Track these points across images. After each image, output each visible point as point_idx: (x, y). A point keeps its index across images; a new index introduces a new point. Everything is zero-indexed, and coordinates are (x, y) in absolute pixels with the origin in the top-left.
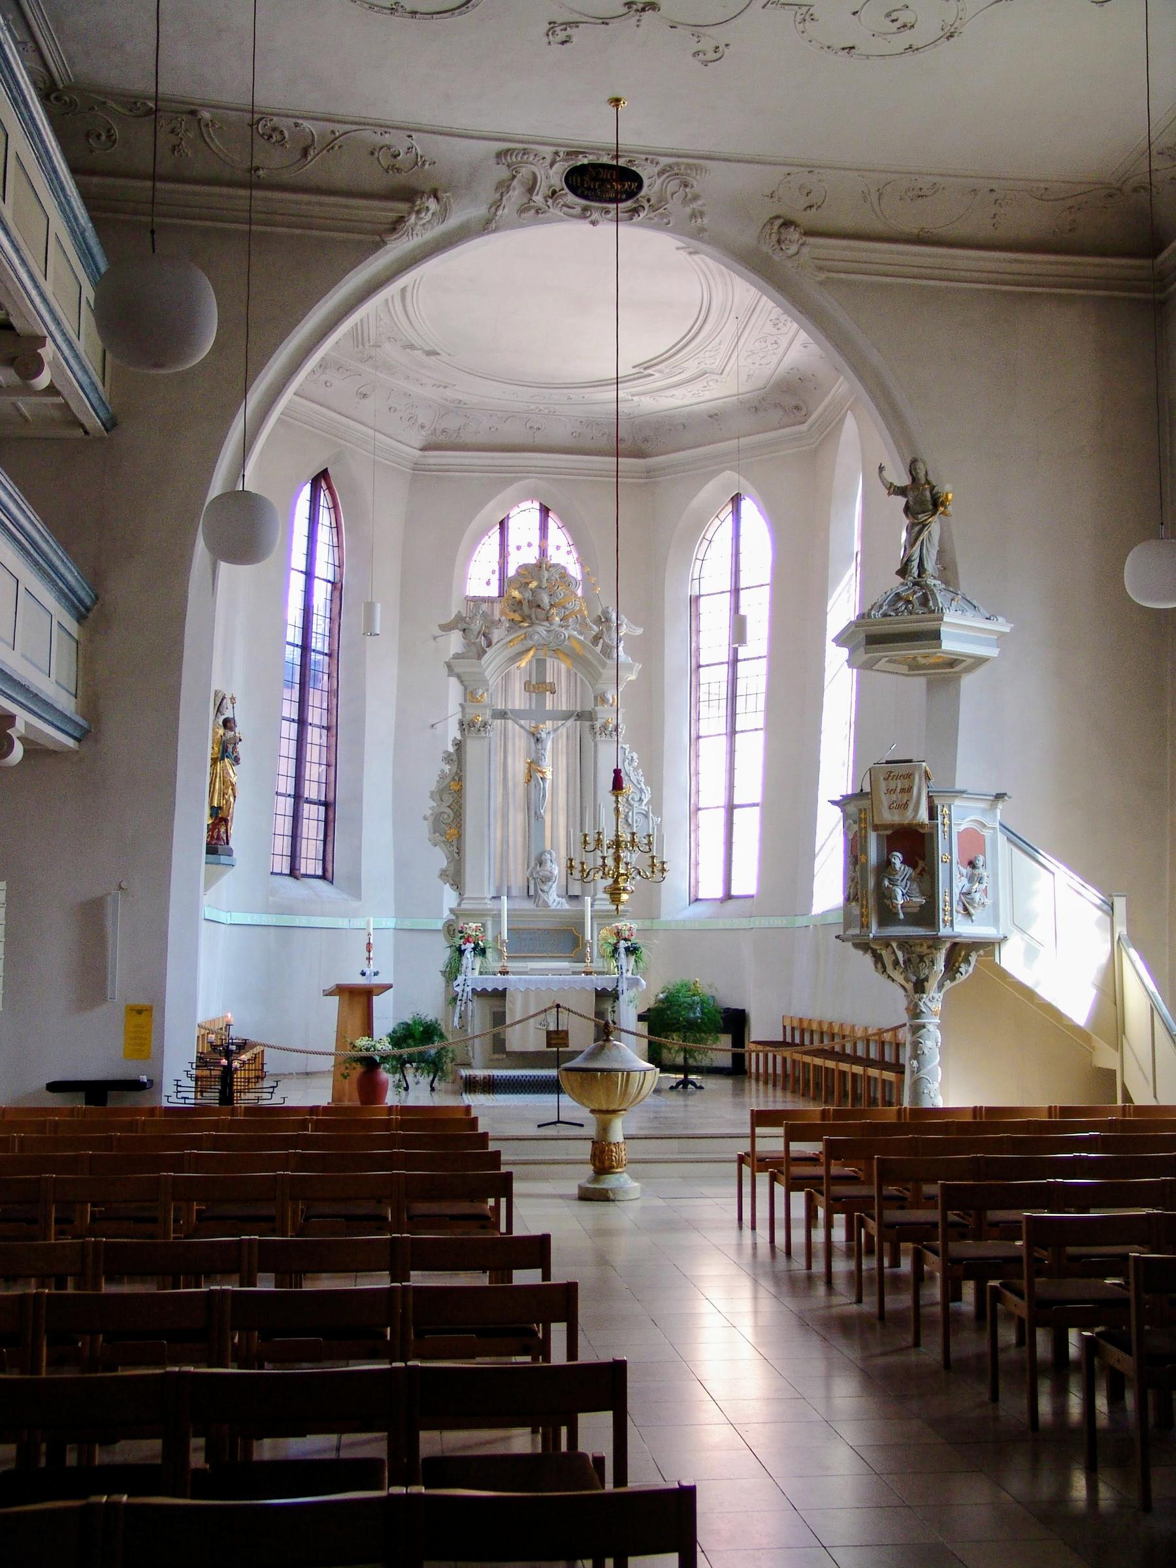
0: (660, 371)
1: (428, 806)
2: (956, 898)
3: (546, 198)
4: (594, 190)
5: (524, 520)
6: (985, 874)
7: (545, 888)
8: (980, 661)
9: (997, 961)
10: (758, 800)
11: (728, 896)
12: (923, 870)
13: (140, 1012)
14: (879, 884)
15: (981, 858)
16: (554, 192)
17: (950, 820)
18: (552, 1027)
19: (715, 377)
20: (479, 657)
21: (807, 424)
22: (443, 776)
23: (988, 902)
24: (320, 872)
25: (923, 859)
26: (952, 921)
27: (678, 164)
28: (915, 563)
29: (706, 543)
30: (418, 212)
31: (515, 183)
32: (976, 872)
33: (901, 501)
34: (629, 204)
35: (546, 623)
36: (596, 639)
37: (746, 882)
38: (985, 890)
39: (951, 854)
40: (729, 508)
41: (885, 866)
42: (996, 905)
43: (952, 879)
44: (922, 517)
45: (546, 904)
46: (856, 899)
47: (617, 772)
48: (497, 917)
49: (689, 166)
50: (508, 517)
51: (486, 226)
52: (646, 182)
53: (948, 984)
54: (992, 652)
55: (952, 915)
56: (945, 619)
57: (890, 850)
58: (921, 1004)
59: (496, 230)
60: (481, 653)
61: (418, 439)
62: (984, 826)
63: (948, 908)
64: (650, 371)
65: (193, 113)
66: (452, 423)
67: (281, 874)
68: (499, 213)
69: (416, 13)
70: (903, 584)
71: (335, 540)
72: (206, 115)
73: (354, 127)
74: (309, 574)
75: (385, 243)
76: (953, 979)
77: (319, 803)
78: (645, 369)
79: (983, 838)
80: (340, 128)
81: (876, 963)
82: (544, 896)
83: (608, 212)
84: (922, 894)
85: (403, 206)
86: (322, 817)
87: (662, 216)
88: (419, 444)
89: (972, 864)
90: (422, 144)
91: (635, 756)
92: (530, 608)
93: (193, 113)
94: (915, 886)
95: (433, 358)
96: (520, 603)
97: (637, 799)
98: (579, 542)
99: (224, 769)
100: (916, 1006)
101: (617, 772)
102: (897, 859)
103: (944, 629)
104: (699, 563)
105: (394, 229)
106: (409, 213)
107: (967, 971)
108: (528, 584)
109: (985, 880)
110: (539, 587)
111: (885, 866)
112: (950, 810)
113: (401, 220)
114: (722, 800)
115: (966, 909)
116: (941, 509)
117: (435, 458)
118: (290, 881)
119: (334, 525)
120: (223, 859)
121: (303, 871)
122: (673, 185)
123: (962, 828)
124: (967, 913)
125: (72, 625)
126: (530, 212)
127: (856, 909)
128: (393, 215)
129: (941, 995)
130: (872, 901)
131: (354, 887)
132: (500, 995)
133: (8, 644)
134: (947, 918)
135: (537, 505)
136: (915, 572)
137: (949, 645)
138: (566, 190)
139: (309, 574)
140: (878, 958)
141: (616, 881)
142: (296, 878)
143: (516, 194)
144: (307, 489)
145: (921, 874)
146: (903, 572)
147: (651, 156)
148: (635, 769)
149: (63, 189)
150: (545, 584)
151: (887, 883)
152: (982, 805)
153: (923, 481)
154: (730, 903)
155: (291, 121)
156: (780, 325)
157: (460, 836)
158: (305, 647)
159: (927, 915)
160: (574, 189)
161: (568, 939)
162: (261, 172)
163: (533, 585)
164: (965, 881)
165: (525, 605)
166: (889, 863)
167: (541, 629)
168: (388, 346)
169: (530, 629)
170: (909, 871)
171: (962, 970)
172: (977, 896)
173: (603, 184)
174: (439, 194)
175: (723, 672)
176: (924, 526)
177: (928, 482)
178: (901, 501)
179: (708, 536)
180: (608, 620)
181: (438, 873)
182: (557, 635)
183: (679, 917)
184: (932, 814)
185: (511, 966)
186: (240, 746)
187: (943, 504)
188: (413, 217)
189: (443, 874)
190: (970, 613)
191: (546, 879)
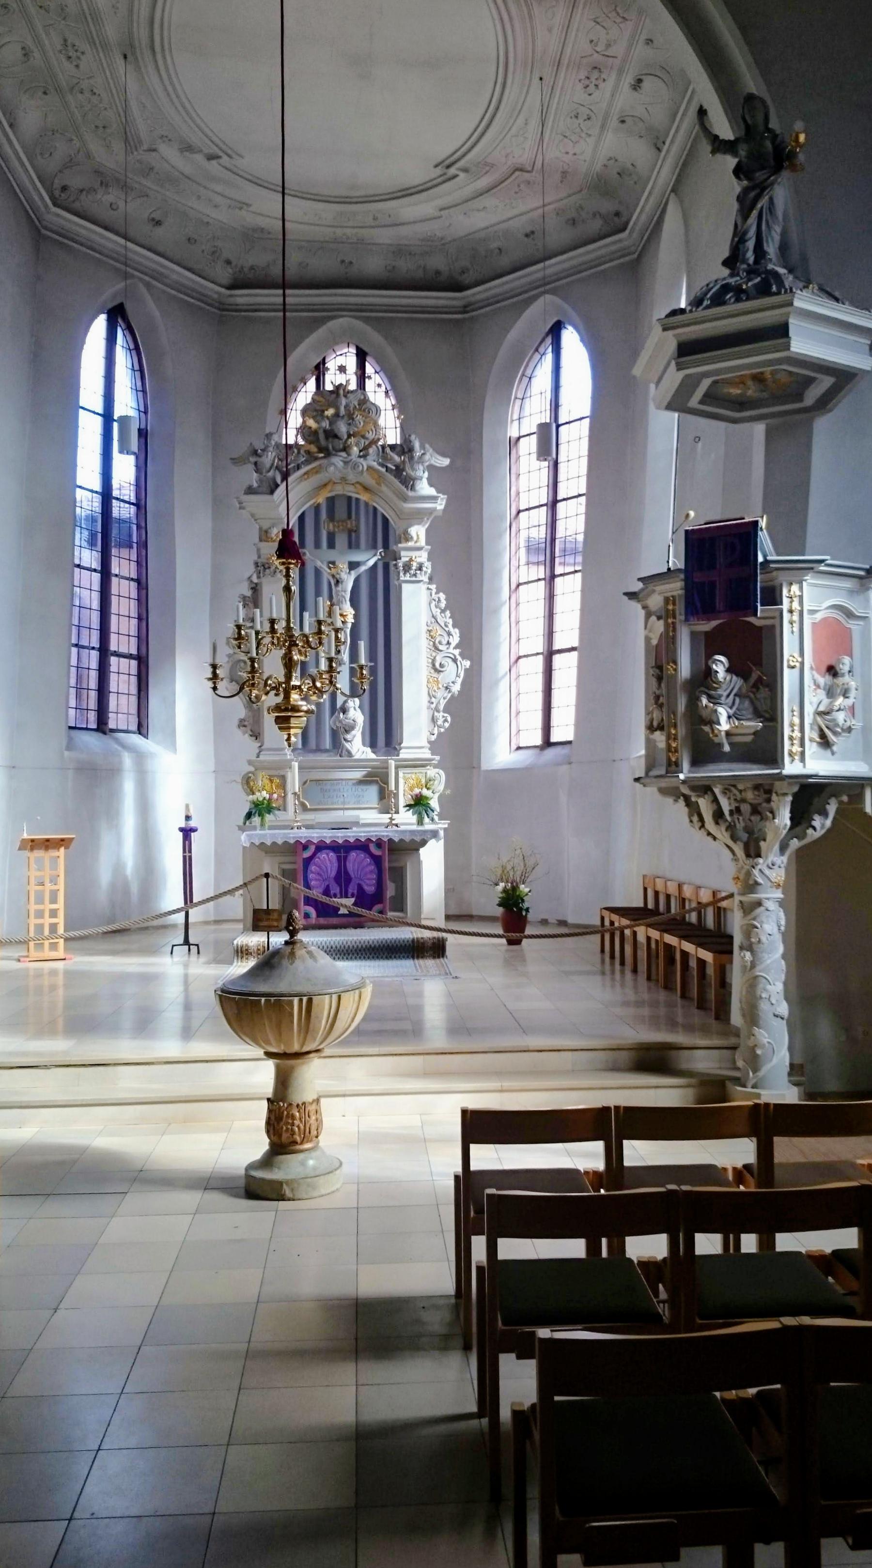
0: (465, 170)
2: (808, 720)
6: (853, 684)
7: (349, 737)
8: (843, 377)
10: (576, 644)
11: (547, 743)
12: (760, 680)
14: (693, 702)
15: (847, 660)
19: (526, 175)
20: (272, 492)
21: (627, 232)
25: (759, 664)
26: (803, 754)
28: (751, 244)
29: (525, 380)
32: (840, 681)
33: (731, 162)
35: (344, 454)
37: (564, 729)
39: (802, 654)
40: (549, 340)
41: (703, 679)
44: (760, 176)
45: (349, 754)
46: (661, 728)
50: (324, 362)
53: (795, 843)
54: (861, 361)
55: (802, 745)
56: (797, 303)
57: (709, 656)
58: (756, 872)
61: (225, 274)
62: (849, 614)
63: (796, 734)
64: (452, 171)
67: (87, 729)
70: (732, 275)
71: (139, 384)
76: (800, 837)
77: (130, 656)
78: (448, 167)
81: (690, 815)
82: (347, 745)
84: (757, 714)
86: (134, 671)
88: (225, 281)
91: (442, 596)
92: (327, 438)
94: (747, 703)
95: (214, 162)
96: (316, 433)
97: (445, 642)
98: (395, 388)
100: (749, 874)
102: (720, 666)
104: (518, 402)
107: (821, 824)
108: (323, 411)
109: (852, 694)
110: (337, 415)
112: (801, 589)
114: (539, 645)
115: (823, 735)
116: (786, 164)
117: (243, 297)
119: (137, 367)
123: (819, 616)
124: (825, 743)
129: (785, 859)
130: (682, 731)
134: (796, 749)
135: (353, 350)
136: (750, 256)
137: (805, 343)
140: (694, 809)
141: (287, 697)
142: (104, 733)
144: (100, 324)
145: (756, 686)
148: (443, 611)
150: (342, 411)
151: (704, 701)
152: (848, 584)
153: (761, 128)
154: (550, 753)
156: (592, 87)
158: (106, 495)
164: (822, 694)
165: (322, 436)
167: (338, 461)
169: (325, 461)
170: (737, 682)
171: (817, 821)
172: (840, 717)
176: (763, 190)
177: (768, 130)
178: (731, 162)
179: (528, 372)
180: (411, 450)
181: (236, 723)
187: (792, 155)
189: (242, 724)
191: (349, 729)
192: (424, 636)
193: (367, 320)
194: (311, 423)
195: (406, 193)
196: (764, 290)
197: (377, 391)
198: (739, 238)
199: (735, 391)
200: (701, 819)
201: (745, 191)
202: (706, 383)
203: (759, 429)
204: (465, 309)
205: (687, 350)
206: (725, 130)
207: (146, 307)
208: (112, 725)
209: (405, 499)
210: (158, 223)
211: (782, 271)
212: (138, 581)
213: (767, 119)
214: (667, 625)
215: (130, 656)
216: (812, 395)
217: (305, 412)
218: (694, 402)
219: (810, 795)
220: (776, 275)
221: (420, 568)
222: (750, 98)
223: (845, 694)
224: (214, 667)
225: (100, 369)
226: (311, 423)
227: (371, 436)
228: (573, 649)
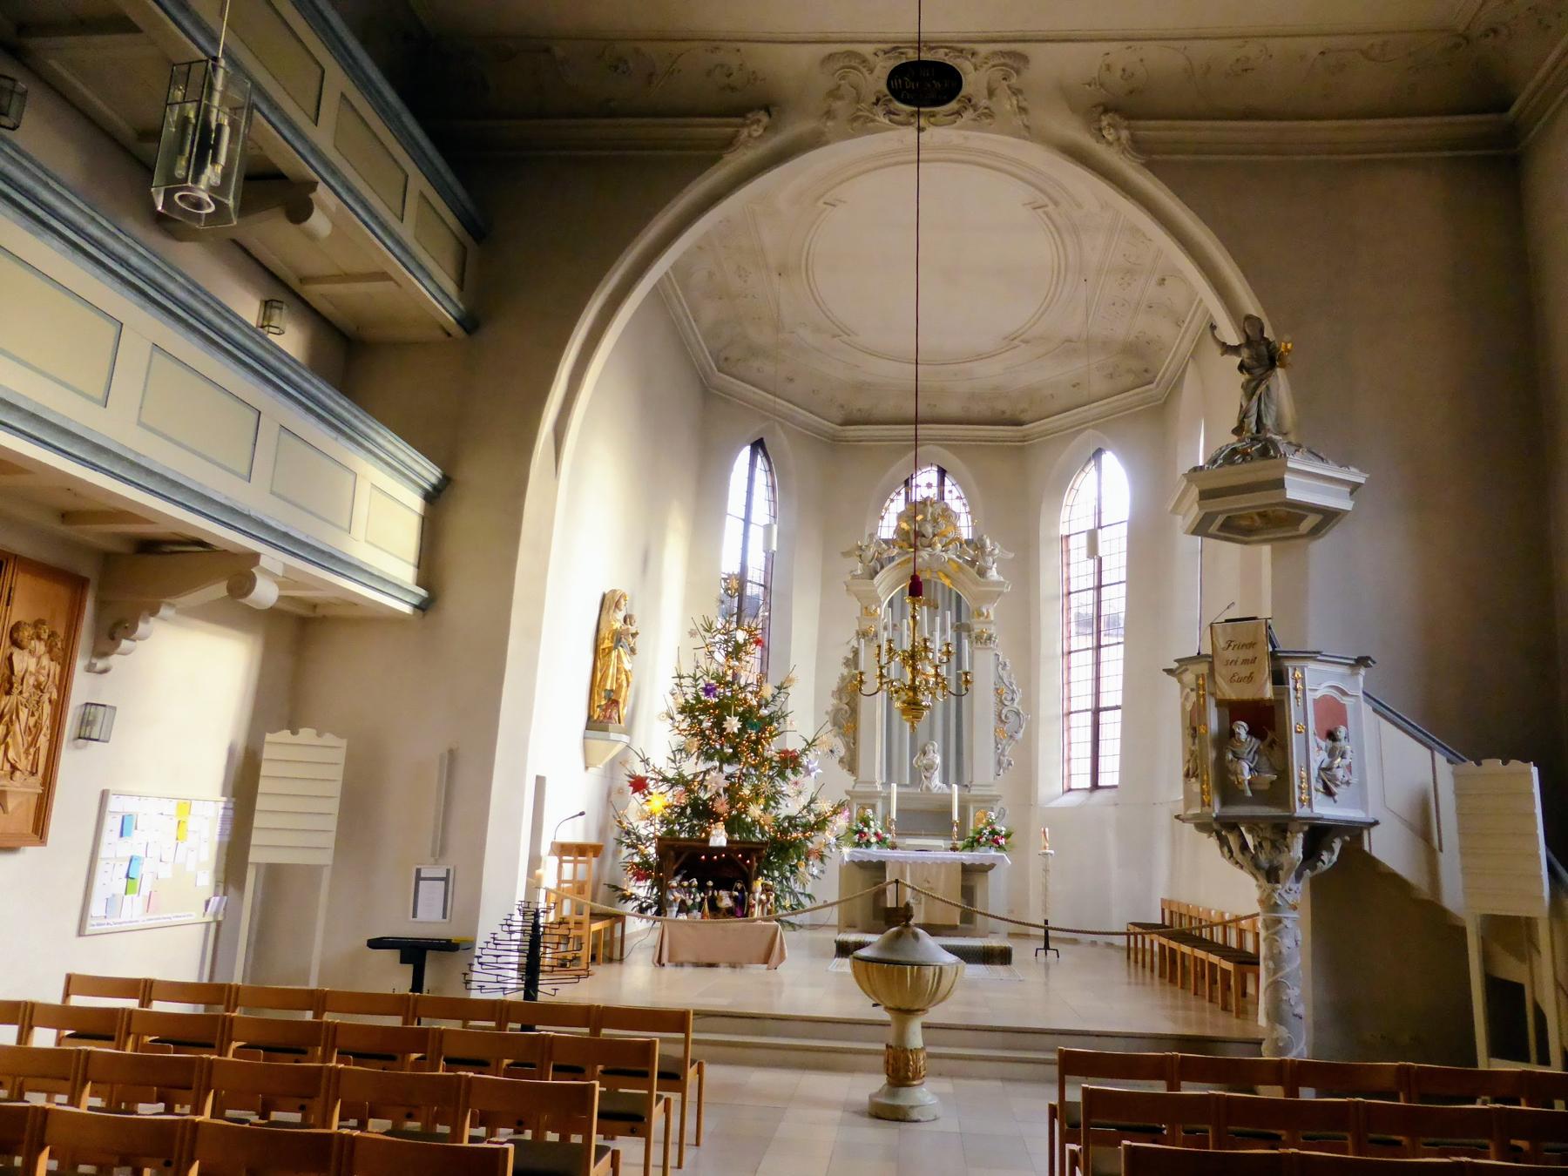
1: (831, 702)
5: (926, 479)
8: (1329, 517)
9: (1366, 848)
11: (1095, 786)
12: (1273, 742)
14: (1220, 758)
15: (1342, 729)
17: (1304, 684)
22: (843, 678)
23: (1354, 780)
25: (1273, 729)
26: (1310, 801)
28: (1253, 419)
34: (953, 105)
36: (972, 563)
38: (1349, 767)
39: (1306, 723)
42: (1362, 785)
43: (1307, 752)
44: (1258, 371)
48: (887, 799)
54: (1345, 504)
55: (1310, 794)
57: (1232, 721)
60: (873, 574)
61: (839, 415)
62: (1344, 693)
65: (547, 50)
66: (862, 404)
72: (559, 52)
74: (747, 521)
75: (720, 157)
76: (1314, 868)
79: (1342, 707)
84: (1273, 769)
85: (738, 120)
89: (1331, 736)
96: (908, 532)
99: (619, 657)
102: (1242, 729)
103: (1287, 477)
107: (1328, 859)
109: (1349, 755)
110: (924, 520)
111: (1226, 738)
114: (1088, 703)
123: (1318, 695)
124: (1328, 792)
126: (860, 124)
127: (1196, 786)
132: (880, 866)
133: (241, 477)
137: (1297, 491)
139: (747, 521)
140: (1223, 842)
144: (746, 452)
146: (1238, 431)
151: (1230, 756)
154: (1099, 794)
157: (855, 730)
159: (1279, 791)
161: (933, 819)
163: (919, 518)
164: (1324, 755)
166: (1232, 734)
170: (1255, 743)
171: (1325, 856)
172: (1340, 773)
173: (925, 84)
175: (1090, 597)
180: (983, 547)
182: (939, 557)
183: (1053, 804)
184: (1279, 678)
185: (898, 841)
190: (1318, 463)
191: (929, 768)
192: (992, 692)
193: (947, 447)
194: (904, 526)
195: (979, 357)
196: (1264, 453)
197: (955, 499)
198: (1244, 415)
199: (1244, 523)
200: (1230, 851)
201: (1249, 382)
202: (1220, 520)
203: (1266, 549)
204: (1024, 439)
205: (1205, 495)
206: (1233, 339)
207: (779, 441)
209: (977, 584)
210: (791, 380)
211: (1277, 438)
213: (1262, 331)
214: (1198, 696)
216: (1305, 526)
217: (900, 517)
218: (1213, 529)
219: (1319, 835)
220: (1274, 444)
221: (990, 638)
222: (1249, 318)
223: (1343, 757)
225: (747, 484)
226: (904, 526)
227: (951, 535)
228: (1117, 708)
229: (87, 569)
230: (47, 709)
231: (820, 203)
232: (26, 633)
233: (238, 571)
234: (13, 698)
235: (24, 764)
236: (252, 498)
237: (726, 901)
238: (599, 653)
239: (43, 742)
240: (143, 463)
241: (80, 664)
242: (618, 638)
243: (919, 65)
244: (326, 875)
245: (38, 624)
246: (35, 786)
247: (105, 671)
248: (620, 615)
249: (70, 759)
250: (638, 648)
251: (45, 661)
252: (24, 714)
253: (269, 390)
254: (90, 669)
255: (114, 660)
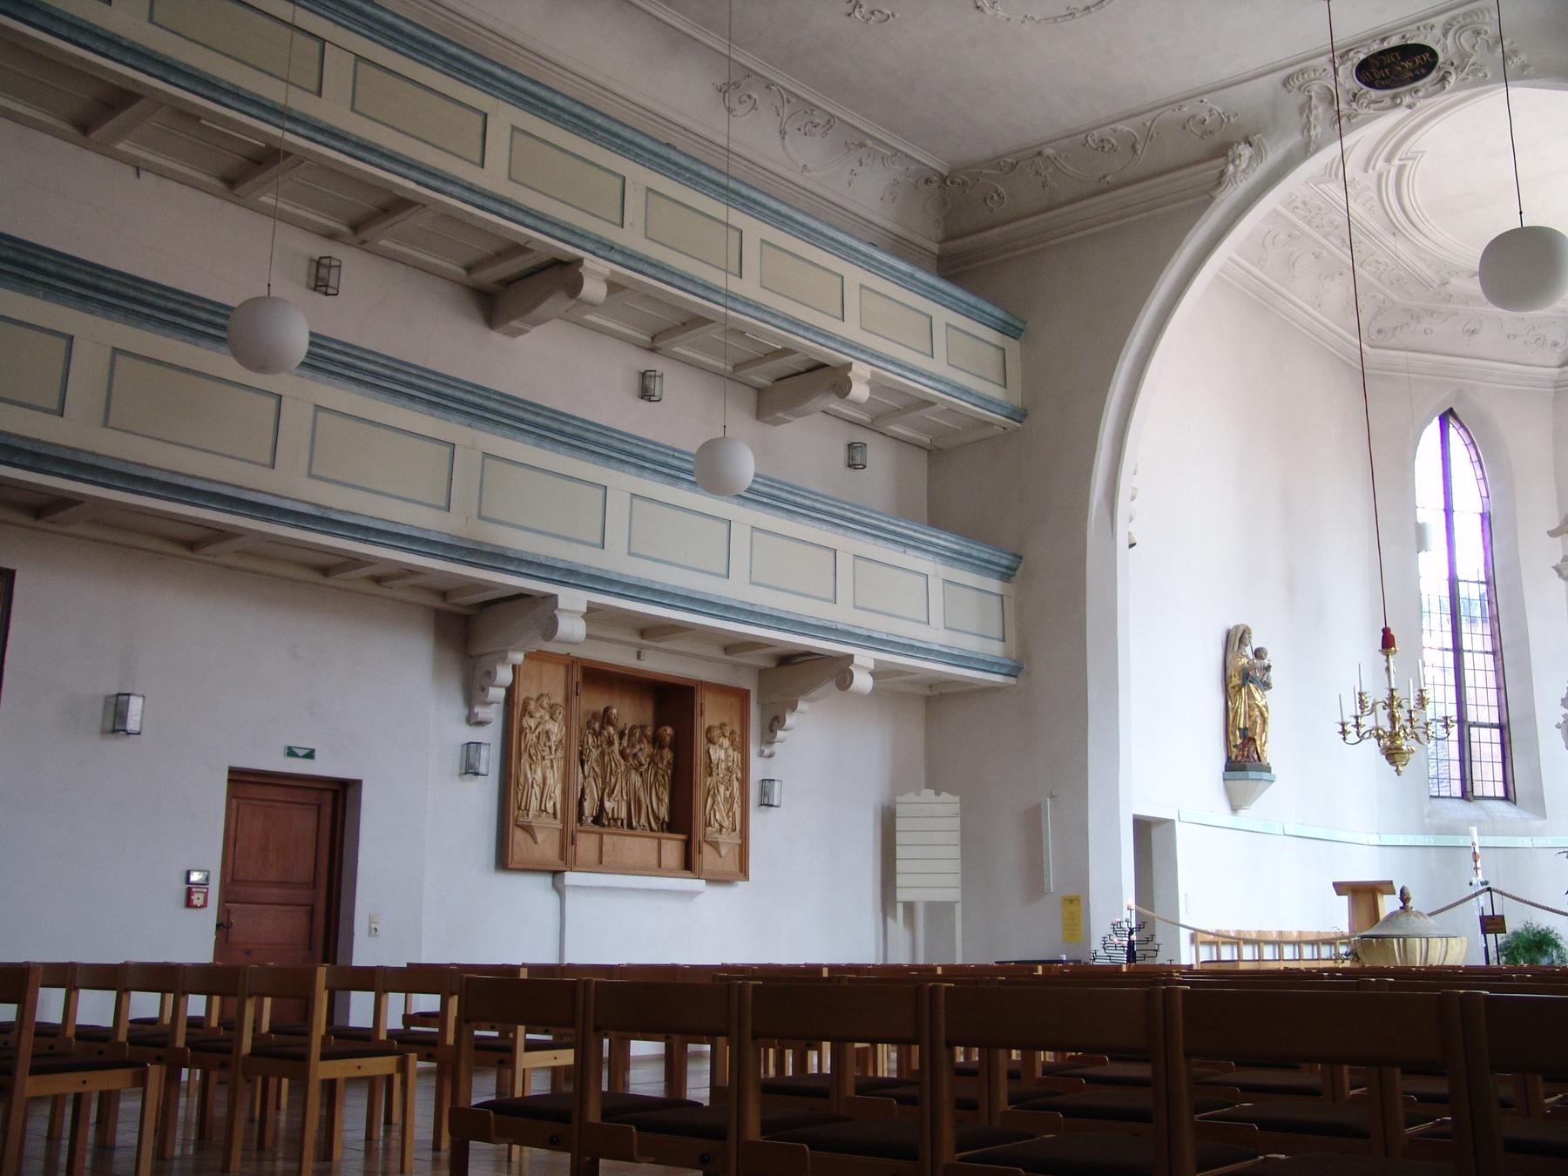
3: (1348, 103)
4: (1387, 77)
13: (1071, 901)
16: (1355, 95)
18: (1488, 912)
24: (1501, 793)
27: (1454, 18)
30: (1233, 162)
31: (1314, 101)
34: (1433, 75)
47: (1386, 631)
49: (1466, 15)
51: (1307, 150)
52: (1438, 49)
59: (1318, 149)
68: (1313, 133)
69: (1088, 8)
72: (1049, 151)
73: (1155, 113)
75: (1213, 198)
77: (1492, 726)
80: (1148, 117)
83: (1417, 91)
85: (1222, 160)
87: (1474, 72)
90: (1215, 105)
93: (1040, 154)
99: (1250, 695)
101: (1386, 631)
105: (1220, 183)
106: (1226, 165)
113: (1222, 173)
118: (1462, 804)
120: (1251, 774)
121: (1478, 792)
122: (1465, 40)
125: (994, 585)
126: (1340, 123)
128: (1216, 171)
131: (1538, 805)
138: (1366, 89)
143: (1320, 111)
147: (1423, 20)
149: (856, 250)
155: (1108, 129)
160: (1371, 85)
162: (1108, 178)
168: (1453, 280)
173: (1397, 67)
174: (1255, 139)
186: (1272, 673)
188: (1231, 168)
208: (1478, 792)
212: (1494, 653)
215: (1492, 726)
224: (1343, 725)
229: (748, 683)
230: (736, 785)
231: (1396, 162)
232: (716, 732)
233: (837, 669)
234: (715, 778)
235: (726, 823)
236: (842, 614)
237: (767, 752)
238: (1229, 691)
239: (737, 808)
240: (756, 609)
241: (753, 750)
242: (1246, 677)
243: (1382, 53)
244: (958, 908)
245: (722, 726)
246: (735, 839)
247: (771, 756)
248: (1248, 651)
249: (756, 818)
250: (1273, 682)
251: (730, 751)
252: (722, 788)
253: (841, 531)
254: (761, 754)
255: (776, 747)
